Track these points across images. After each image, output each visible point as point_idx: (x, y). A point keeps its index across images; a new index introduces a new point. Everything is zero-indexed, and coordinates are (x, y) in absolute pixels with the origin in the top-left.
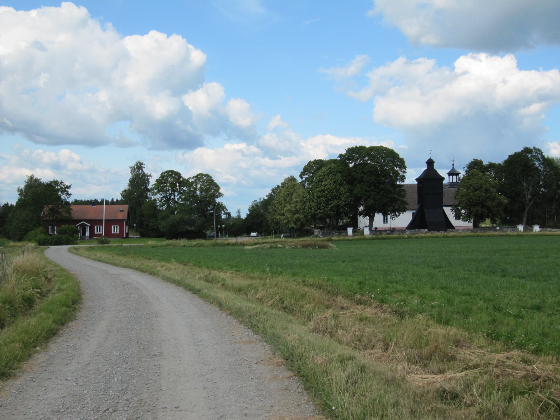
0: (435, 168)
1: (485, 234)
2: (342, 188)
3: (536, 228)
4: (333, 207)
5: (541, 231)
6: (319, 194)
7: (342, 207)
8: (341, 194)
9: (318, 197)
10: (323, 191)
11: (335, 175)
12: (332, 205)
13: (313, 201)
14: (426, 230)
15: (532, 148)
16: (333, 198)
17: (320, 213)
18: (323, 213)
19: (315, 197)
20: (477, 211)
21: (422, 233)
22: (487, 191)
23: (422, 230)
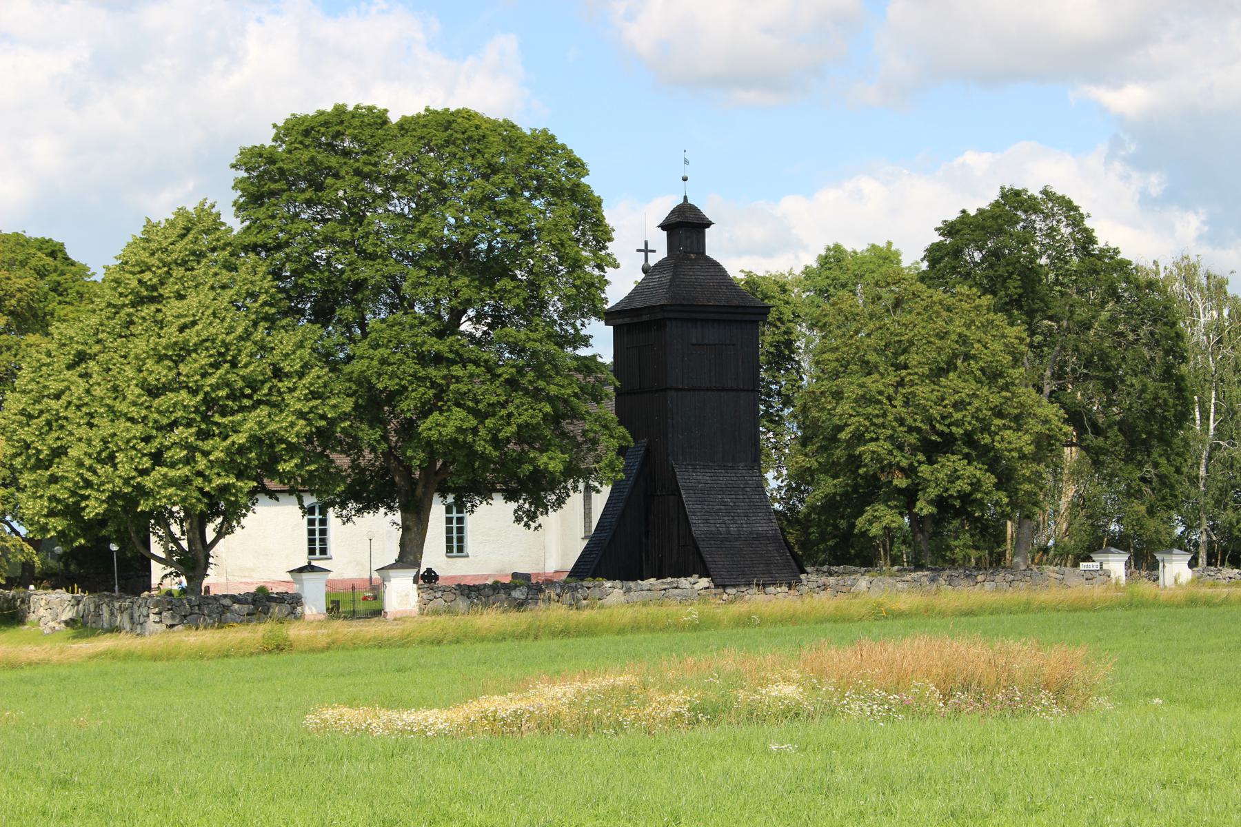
0: (709, 252)
1: (1044, 596)
2: (284, 341)
3: (1176, 570)
4: (242, 450)
5: (1196, 581)
6: (160, 373)
7: (292, 449)
8: (278, 373)
9: (154, 392)
10: (182, 353)
11: (232, 268)
12: (241, 439)
13: (115, 415)
14: (704, 582)
15: (1035, 191)
16: (246, 395)
17: (171, 483)
18: (187, 481)
19: (133, 392)
20: (954, 477)
21: (684, 600)
22: (992, 376)
23: (684, 582)
